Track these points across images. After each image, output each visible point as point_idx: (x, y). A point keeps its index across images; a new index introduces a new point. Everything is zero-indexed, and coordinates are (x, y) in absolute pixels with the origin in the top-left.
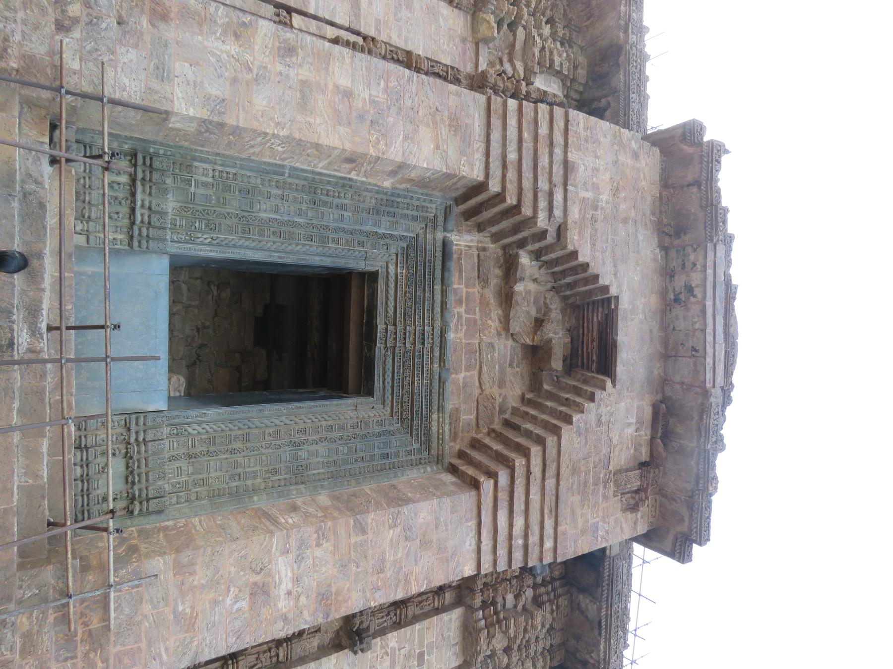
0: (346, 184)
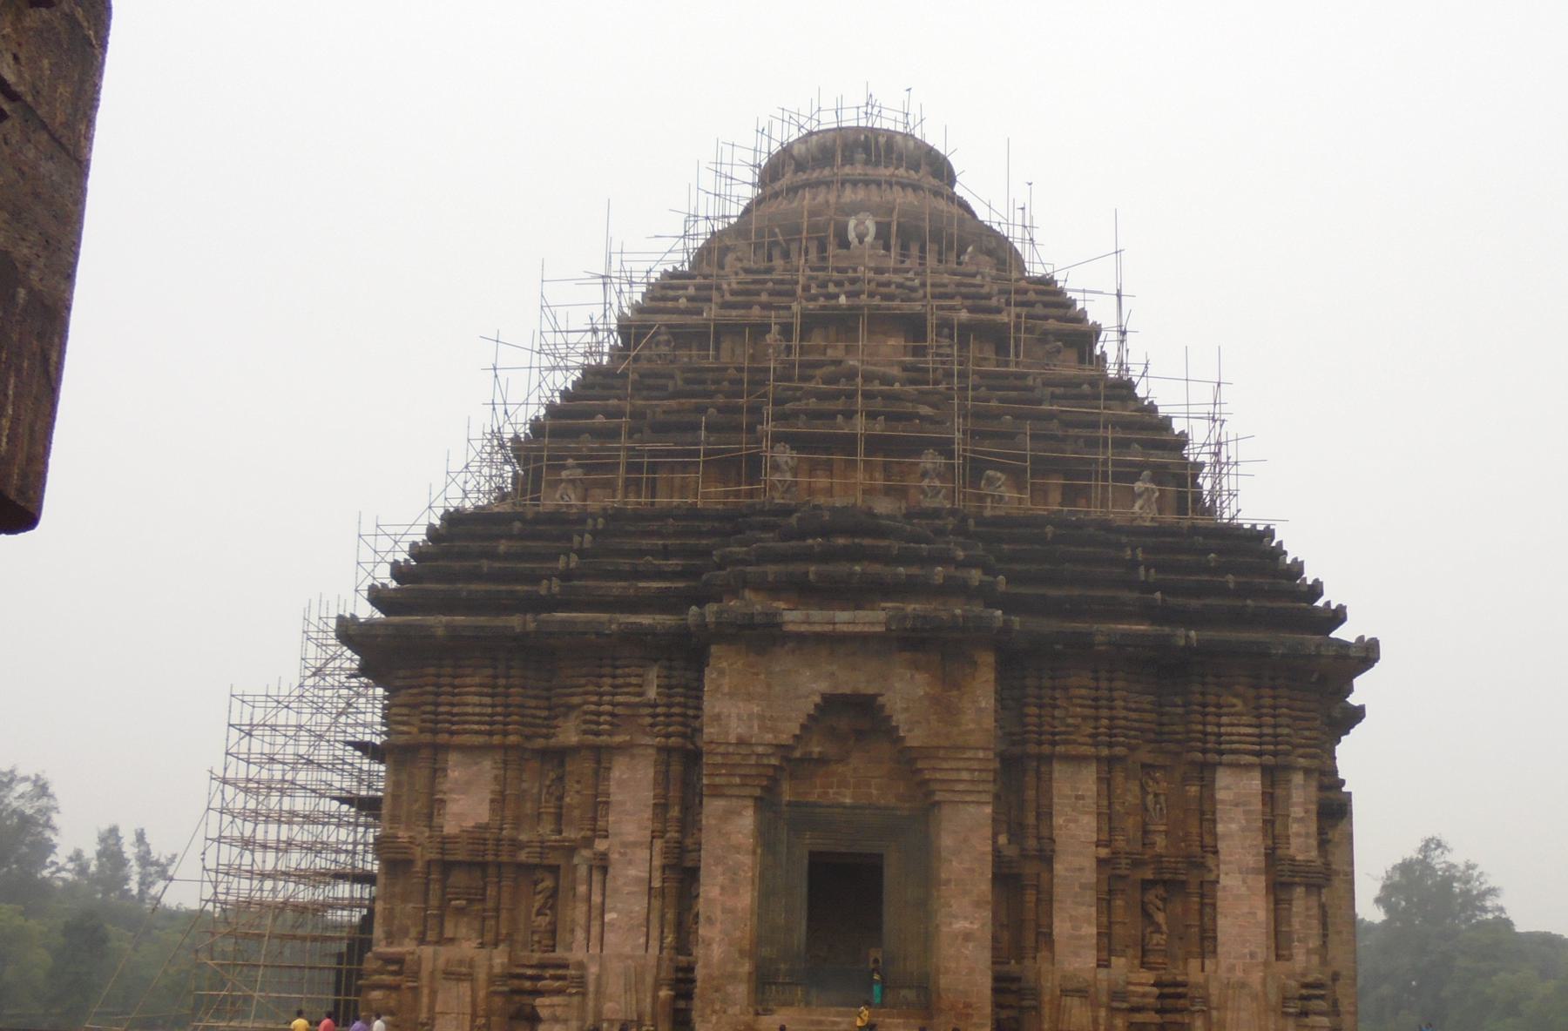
0: (762, 876)
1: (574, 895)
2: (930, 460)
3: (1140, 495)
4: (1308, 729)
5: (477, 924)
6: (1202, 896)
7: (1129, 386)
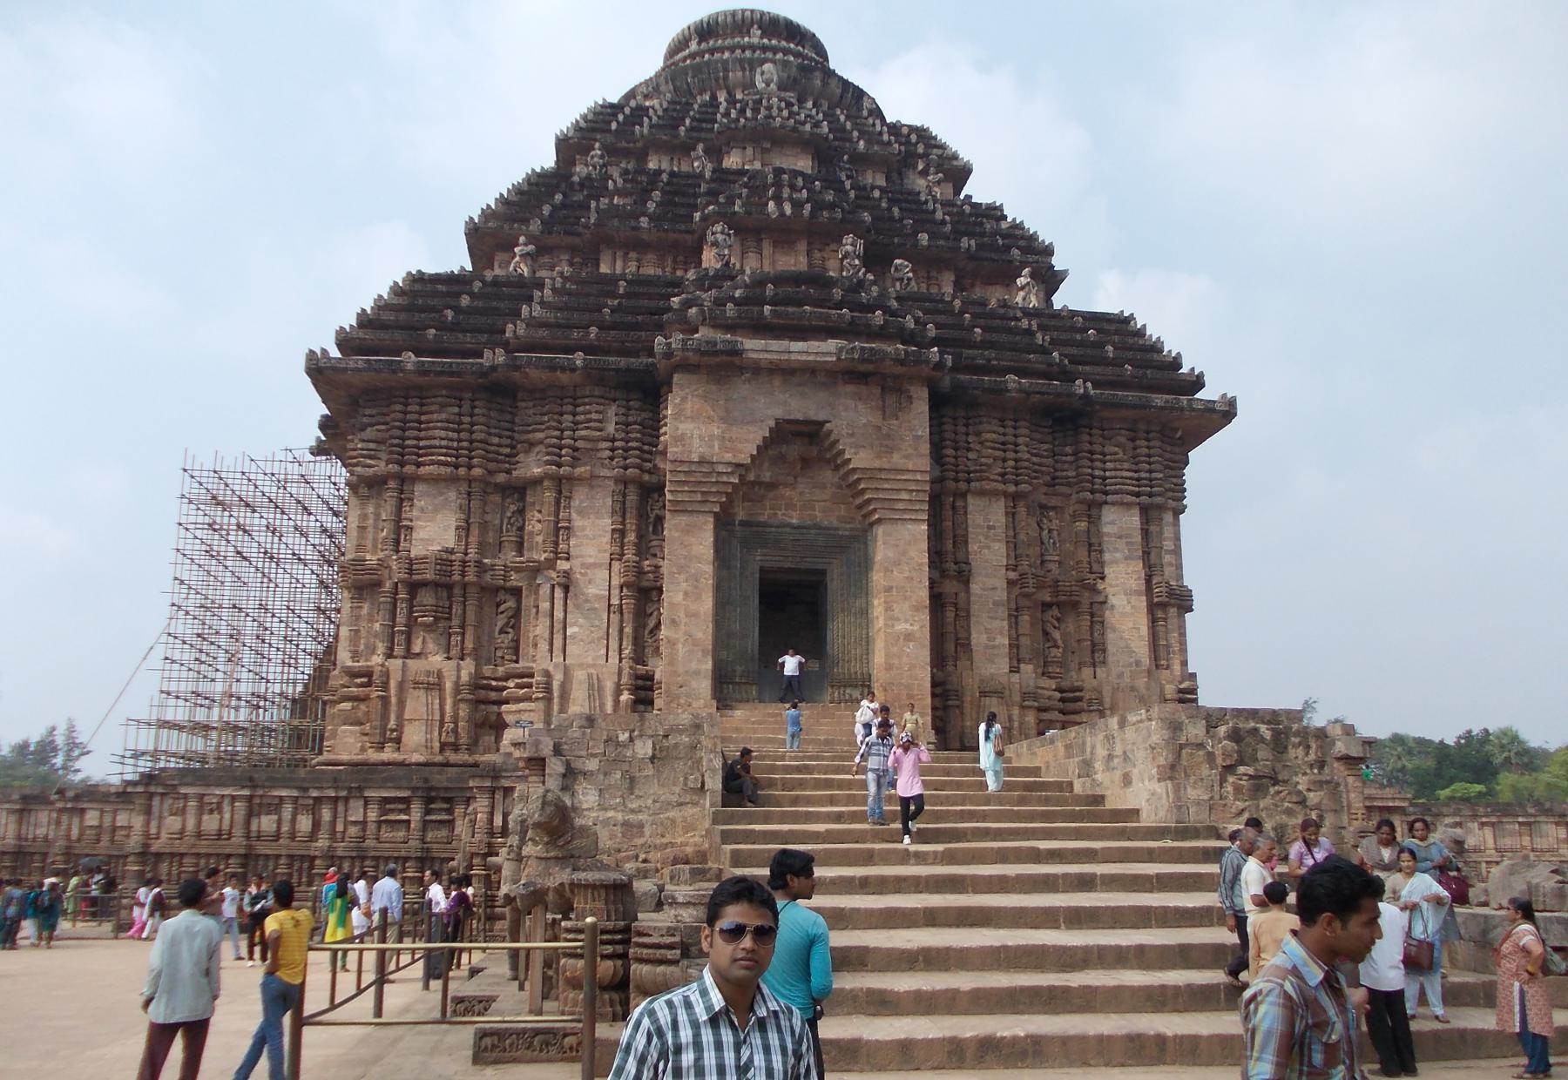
1: (537, 612)
2: (850, 243)
3: (1022, 288)
4: (1175, 477)
5: (443, 641)
6: (1092, 615)
7: (1000, 208)
